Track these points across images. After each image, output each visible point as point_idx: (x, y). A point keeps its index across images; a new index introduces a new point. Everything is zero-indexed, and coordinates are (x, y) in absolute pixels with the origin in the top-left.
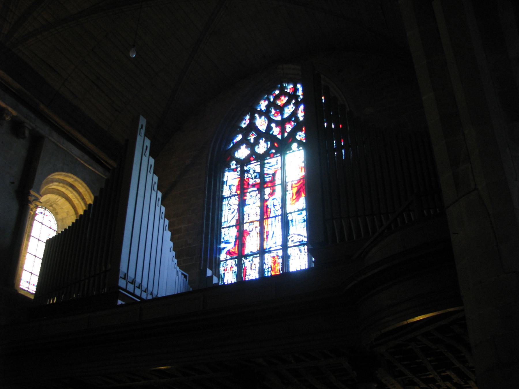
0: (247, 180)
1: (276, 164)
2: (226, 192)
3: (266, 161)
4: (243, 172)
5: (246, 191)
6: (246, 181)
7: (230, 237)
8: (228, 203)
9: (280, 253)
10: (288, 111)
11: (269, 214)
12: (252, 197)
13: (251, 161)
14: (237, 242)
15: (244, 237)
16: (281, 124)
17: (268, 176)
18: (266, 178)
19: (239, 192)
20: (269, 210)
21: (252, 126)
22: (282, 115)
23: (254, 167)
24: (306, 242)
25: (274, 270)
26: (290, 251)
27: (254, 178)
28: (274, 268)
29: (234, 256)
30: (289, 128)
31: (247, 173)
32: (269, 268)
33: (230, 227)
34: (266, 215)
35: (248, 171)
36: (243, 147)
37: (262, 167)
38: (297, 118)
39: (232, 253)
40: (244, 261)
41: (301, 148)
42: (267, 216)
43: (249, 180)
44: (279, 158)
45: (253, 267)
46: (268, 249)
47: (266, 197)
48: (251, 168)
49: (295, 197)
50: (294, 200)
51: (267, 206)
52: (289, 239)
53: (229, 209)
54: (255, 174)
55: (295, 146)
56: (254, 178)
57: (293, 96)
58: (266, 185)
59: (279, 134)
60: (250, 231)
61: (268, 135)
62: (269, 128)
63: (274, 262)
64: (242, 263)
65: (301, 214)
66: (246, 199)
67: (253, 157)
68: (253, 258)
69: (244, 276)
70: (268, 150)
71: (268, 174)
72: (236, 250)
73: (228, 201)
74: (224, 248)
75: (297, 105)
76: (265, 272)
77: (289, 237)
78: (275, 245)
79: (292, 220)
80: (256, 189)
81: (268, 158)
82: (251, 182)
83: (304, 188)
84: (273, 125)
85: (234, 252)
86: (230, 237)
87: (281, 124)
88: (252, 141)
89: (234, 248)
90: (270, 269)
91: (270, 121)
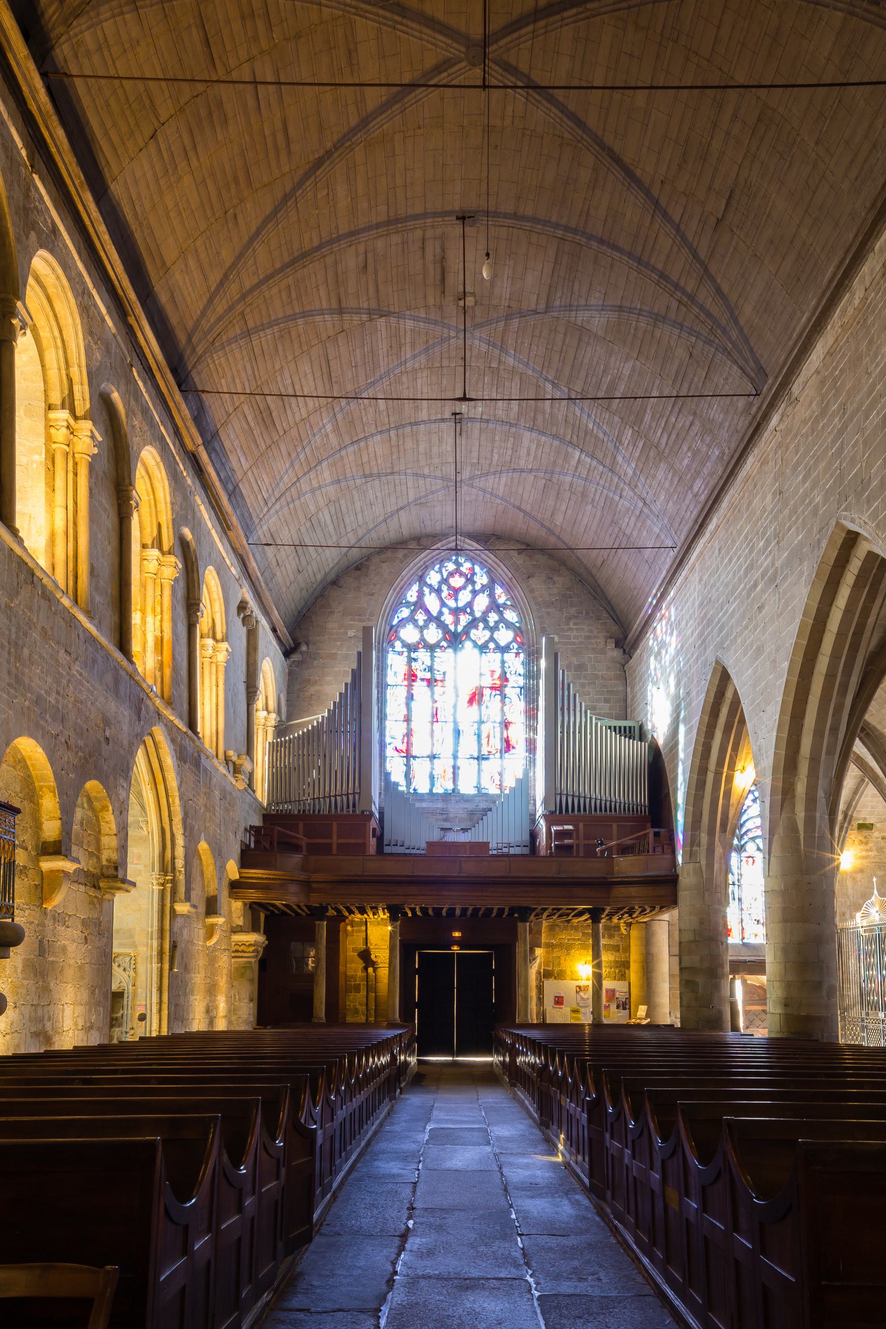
2: (390, 679)
4: (411, 660)
10: (465, 597)
13: (419, 648)
16: (456, 612)
21: (419, 604)
22: (456, 600)
23: (423, 655)
26: (459, 763)
30: (464, 619)
35: (415, 660)
36: (410, 627)
37: (432, 658)
38: (472, 613)
44: (453, 655)
54: (424, 666)
55: (468, 644)
57: (470, 580)
61: (437, 620)
62: (441, 613)
70: (439, 642)
75: (475, 593)
87: (456, 612)
88: (421, 623)
91: (443, 604)
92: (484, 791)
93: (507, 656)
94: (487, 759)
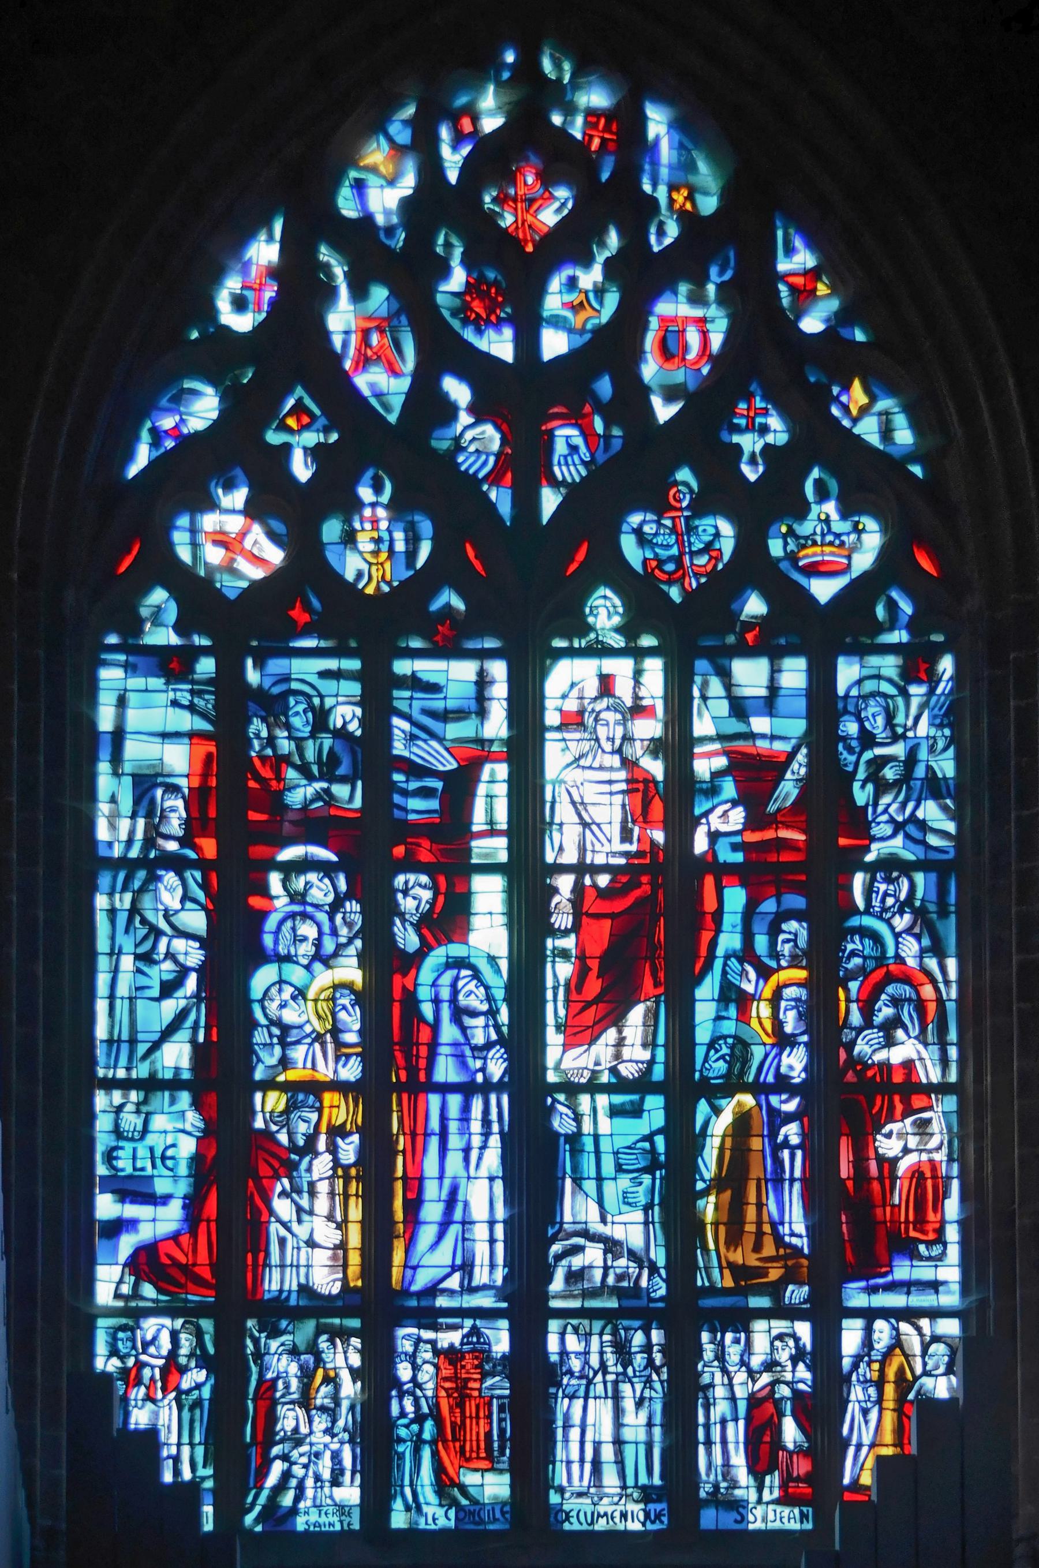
0: (266, 773)
1: (473, 705)
3: (402, 667)
5: (258, 851)
6: (257, 777)
8: (134, 910)
11: (422, 1063)
12: (309, 909)
15: (258, 1180)
17: (413, 785)
18: (405, 793)
19: (209, 847)
20: (425, 1035)
27: (315, 769)
32: (420, 1419)
33: (151, 1085)
40: (256, 1342)
42: (412, 1070)
43: (280, 778)
46: (420, 1294)
48: (295, 685)
49: (594, 987)
51: (411, 1000)
52: (558, 1258)
56: (315, 769)
58: (399, 851)
65: (636, 1111)
66: (264, 914)
73: (128, 897)
78: (454, 1282)
79: (575, 1139)
81: (416, 643)
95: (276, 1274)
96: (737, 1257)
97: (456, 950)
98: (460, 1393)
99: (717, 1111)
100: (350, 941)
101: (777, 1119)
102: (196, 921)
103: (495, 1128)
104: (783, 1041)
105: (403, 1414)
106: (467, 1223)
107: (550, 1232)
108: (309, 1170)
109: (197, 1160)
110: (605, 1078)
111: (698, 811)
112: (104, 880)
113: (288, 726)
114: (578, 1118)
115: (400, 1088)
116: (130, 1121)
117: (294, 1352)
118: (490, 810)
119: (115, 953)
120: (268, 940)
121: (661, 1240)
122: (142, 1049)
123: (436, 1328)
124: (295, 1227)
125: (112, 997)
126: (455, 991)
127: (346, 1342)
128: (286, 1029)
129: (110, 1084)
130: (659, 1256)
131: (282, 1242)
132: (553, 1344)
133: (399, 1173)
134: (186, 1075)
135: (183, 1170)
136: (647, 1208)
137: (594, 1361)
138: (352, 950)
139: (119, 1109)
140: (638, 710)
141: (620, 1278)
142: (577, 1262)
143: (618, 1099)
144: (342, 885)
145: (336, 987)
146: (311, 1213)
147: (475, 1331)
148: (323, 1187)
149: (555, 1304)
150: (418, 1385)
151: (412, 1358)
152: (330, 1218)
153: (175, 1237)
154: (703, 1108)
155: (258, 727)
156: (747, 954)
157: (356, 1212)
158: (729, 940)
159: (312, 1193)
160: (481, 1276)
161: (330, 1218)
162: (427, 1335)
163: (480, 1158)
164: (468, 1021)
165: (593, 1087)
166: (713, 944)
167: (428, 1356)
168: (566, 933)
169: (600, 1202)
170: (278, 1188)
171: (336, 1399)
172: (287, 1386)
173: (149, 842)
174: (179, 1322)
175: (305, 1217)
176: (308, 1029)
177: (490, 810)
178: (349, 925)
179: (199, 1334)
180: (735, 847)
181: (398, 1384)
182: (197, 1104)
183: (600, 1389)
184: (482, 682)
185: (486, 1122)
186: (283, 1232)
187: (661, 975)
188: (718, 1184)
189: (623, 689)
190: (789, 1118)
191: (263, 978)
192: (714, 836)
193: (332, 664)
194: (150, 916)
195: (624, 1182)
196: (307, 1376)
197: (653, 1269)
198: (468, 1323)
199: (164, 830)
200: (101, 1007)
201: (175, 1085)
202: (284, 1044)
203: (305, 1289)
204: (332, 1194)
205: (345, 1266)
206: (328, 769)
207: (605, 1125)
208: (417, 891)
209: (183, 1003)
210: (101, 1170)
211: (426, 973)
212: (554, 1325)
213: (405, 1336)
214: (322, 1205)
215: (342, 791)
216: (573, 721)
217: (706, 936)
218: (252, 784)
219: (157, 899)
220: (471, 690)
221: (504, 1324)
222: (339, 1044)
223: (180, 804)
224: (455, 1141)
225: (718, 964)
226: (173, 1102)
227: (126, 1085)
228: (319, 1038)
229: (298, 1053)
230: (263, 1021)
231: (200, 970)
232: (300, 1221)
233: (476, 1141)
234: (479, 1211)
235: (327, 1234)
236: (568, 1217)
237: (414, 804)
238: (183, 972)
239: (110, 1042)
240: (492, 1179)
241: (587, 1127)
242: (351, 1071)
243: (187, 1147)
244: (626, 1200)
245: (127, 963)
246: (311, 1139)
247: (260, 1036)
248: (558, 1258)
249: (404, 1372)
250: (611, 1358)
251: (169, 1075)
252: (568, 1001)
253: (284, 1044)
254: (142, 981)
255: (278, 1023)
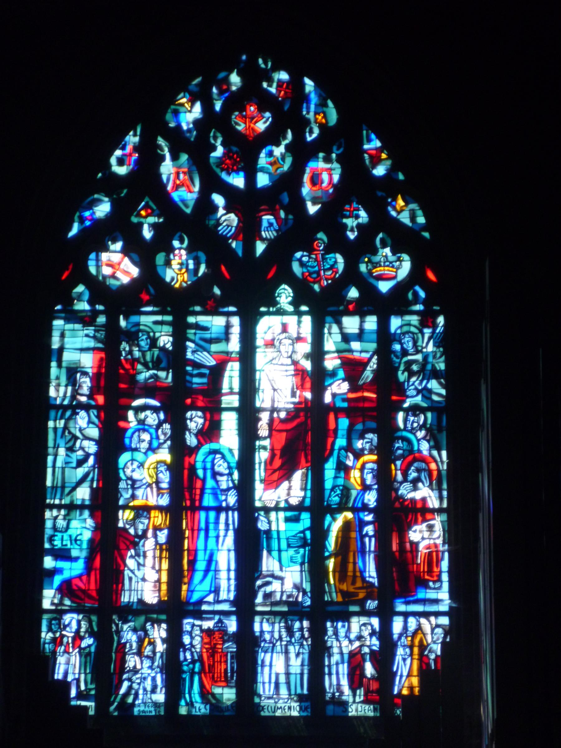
0: (127, 366)
1: (223, 336)
3: (191, 320)
5: (123, 401)
6: (124, 368)
7: (73, 538)
8: (66, 428)
9: (232, 625)
11: (197, 497)
12: (146, 427)
14: (97, 562)
15: (119, 550)
17: (195, 372)
18: (192, 376)
19: (101, 399)
20: (199, 484)
24: (308, 609)
25: (210, 672)
27: (150, 365)
28: (209, 665)
29: (86, 605)
31: (127, 343)
32: (193, 662)
33: (71, 507)
34: (187, 495)
39: (80, 594)
40: (117, 625)
41: (304, 308)
42: (193, 501)
43: (134, 368)
45: (148, 651)
47: (191, 440)
48: (142, 327)
49: (278, 463)
50: (275, 471)
51: (193, 469)
52: (260, 587)
53: (68, 446)
56: (150, 365)
58: (189, 401)
59: (235, 237)
60: (137, 535)
63: (211, 648)
64: (112, 632)
65: (296, 520)
66: (125, 430)
67: (148, 292)
68: (146, 622)
69: (117, 671)
71: (197, 365)
72: (93, 586)
73: (63, 422)
74: (55, 571)
76: (184, 672)
77: (259, 583)
78: (210, 598)
79: (268, 532)
80: (158, 404)
81: (198, 308)
82: (144, 375)
83: (309, 439)
84: (218, 200)
85: (84, 591)
86: (73, 542)
88: (147, 234)
89: (84, 578)
90: (197, 665)
92: (330, 710)
93: (395, 323)
94: (346, 617)
95: (127, 593)
96: (344, 587)
97: (213, 446)
98: (213, 651)
99: (334, 519)
100: (165, 442)
101: (362, 524)
102: (94, 432)
103: (231, 527)
104: (366, 488)
105: (186, 659)
106: (216, 571)
107: (256, 575)
108: (143, 546)
109: (91, 542)
110: (282, 505)
111: (326, 384)
112: (52, 413)
113: (138, 345)
114: (269, 523)
115: (186, 509)
116: (61, 523)
117: (135, 630)
118: (231, 383)
119: (56, 447)
120: (127, 441)
121: (308, 579)
122: (67, 490)
123: (202, 619)
124: (136, 572)
125: (54, 467)
126: (213, 465)
127: (159, 626)
128: (134, 481)
129: (52, 507)
130: (307, 586)
131: (130, 579)
132: (257, 628)
133: (186, 547)
134: (87, 503)
135: (85, 546)
136: (302, 564)
137: (276, 635)
138: (166, 446)
139: (57, 517)
140: (299, 339)
141: (289, 596)
142: (268, 589)
143: (289, 514)
144: (162, 416)
145: (158, 462)
146: (144, 565)
147: (220, 621)
148: (150, 554)
149: (259, 609)
150: (192, 646)
151: (190, 633)
152: (153, 568)
153: (80, 577)
154: (328, 518)
155: (125, 346)
156: (349, 448)
157: (165, 565)
158: (341, 442)
159: (145, 556)
160: (223, 596)
161: (153, 568)
162: (197, 622)
163: (224, 541)
164: (219, 478)
165: (277, 509)
166: (333, 444)
167: (198, 632)
168: (265, 438)
169: (280, 561)
170: (129, 554)
171: (154, 652)
172: (131, 646)
173: (73, 397)
174: (81, 617)
175: (141, 568)
176: (144, 481)
177: (231, 383)
178: (165, 434)
179: (90, 622)
180: (344, 400)
181: (183, 645)
182: (92, 516)
183: (279, 648)
184: (228, 327)
185: (227, 524)
186: (131, 575)
187: (309, 457)
188: (335, 554)
189: (293, 331)
190: (368, 523)
191: (124, 458)
192: (334, 395)
193: (159, 318)
194: (73, 430)
195: (291, 552)
196: (140, 641)
197: (305, 593)
198: (217, 617)
199: (80, 392)
200: (49, 471)
201: (82, 507)
202: (133, 488)
203: (141, 601)
204: (154, 557)
205: (159, 590)
206: (157, 364)
207: (283, 526)
208: (197, 419)
209: (86, 470)
210: (47, 546)
211: (200, 457)
212: (257, 619)
213: (187, 623)
214: (149, 561)
215: (162, 374)
216: (270, 344)
217: (330, 440)
218: (122, 371)
219: (76, 423)
220: (223, 330)
221: (234, 618)
222: (159, 489)
223: (88, 380)
224: (212, 533)
225: (336, 453)
226: (81, 515)
227: (59, 507)
228: (150, 485)
229: (139, 493)
230: (123, 477)
231: (96, 455)
232: (139, 569)
233: (222, 533)
234: (223, 566)
235: (152, 576)
236: (264, 568)
237: (196, 380)
238: (87, 456)
239: (53, 487)
240: (229, 550)
241: (274, 527)
242: (164, 501)
243: (87, 535)
244: (292, 560)
245: (62, 451)
246: (145, 532)
247: (122, 485)
248: (260, 587)
249: (186, 640)
250: (284, 634)
251: (79, 502)
252: (266, 470)
253: (133, 488)
254: (69, 460)
255: (130, 478)
